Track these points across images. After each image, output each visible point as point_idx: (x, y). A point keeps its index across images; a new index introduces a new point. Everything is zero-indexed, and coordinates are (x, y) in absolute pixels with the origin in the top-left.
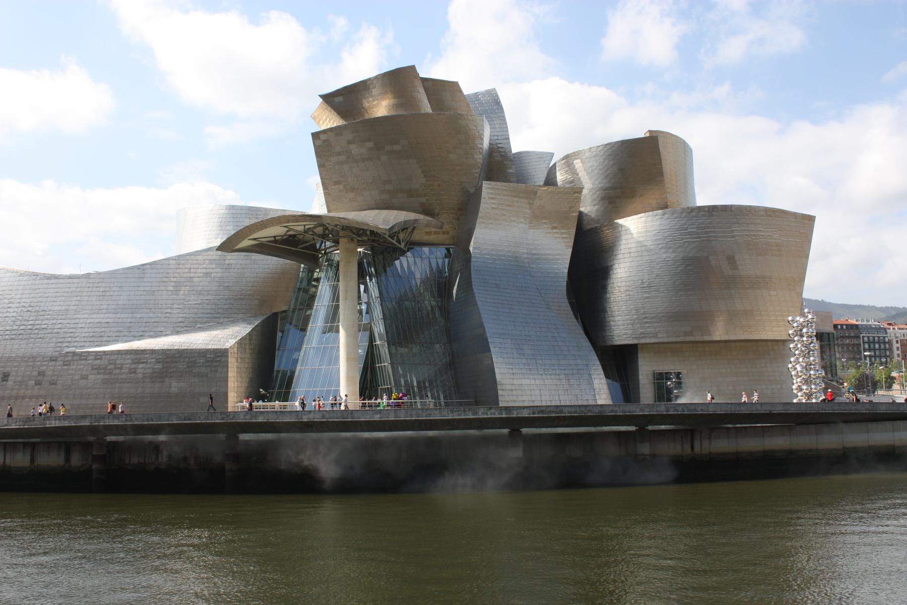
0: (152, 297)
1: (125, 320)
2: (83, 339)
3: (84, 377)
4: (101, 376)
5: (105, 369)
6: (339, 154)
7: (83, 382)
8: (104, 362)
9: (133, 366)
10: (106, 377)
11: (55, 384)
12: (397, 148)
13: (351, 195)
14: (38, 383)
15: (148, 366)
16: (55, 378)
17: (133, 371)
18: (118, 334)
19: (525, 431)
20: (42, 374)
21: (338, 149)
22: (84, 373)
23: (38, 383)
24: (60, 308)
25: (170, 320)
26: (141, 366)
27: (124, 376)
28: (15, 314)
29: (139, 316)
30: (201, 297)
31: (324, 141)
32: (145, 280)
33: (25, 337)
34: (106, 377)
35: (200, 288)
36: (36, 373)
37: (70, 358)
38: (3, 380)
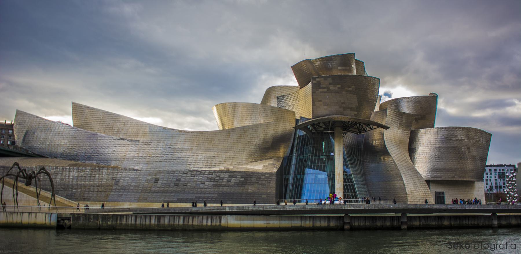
3: (203, 183)
4: (212, 183)
5: (214, 179)
6: (324, 88)
7: (202, 186)
8: (214, 176)
9: (229, 179)
11: (186, 186)
12: (350, 89)
13: (326, 107)
14: (177, 185)
16: (186, 182)
17: (229, 181)
19: (498, 214)
20: (179, 180)
21: (324, 86)
23: (177, 185)
24: (187, 148)
26: (233, 179)
27: (225, 183)
28: (161, 149)
29: (229, 154)
31: (318, 81)
33: (168, 161)
36: (175, 180)
37: (195, 173)
38: (155, 183)
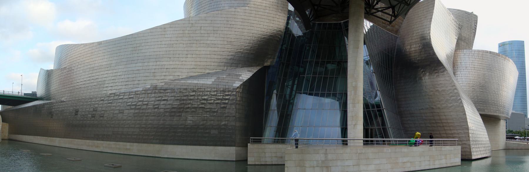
0: (171, 49)
1: (150, 67)
2: (120, 84)
3: (121, 112)
4: (133, 111)
5: (136, 105)
7: (120, 115)
10: (137, 111)
11: (103, 117)
15: (169, 102)
16: (103, 112)
18: (145, 78)
22: (121, 108)
25: (185, 67)
26: (163, 103)
27: (149, 111)
30: (210, 49)
32: (166, 36)
34: (137, 111)
35: (208, 42)
